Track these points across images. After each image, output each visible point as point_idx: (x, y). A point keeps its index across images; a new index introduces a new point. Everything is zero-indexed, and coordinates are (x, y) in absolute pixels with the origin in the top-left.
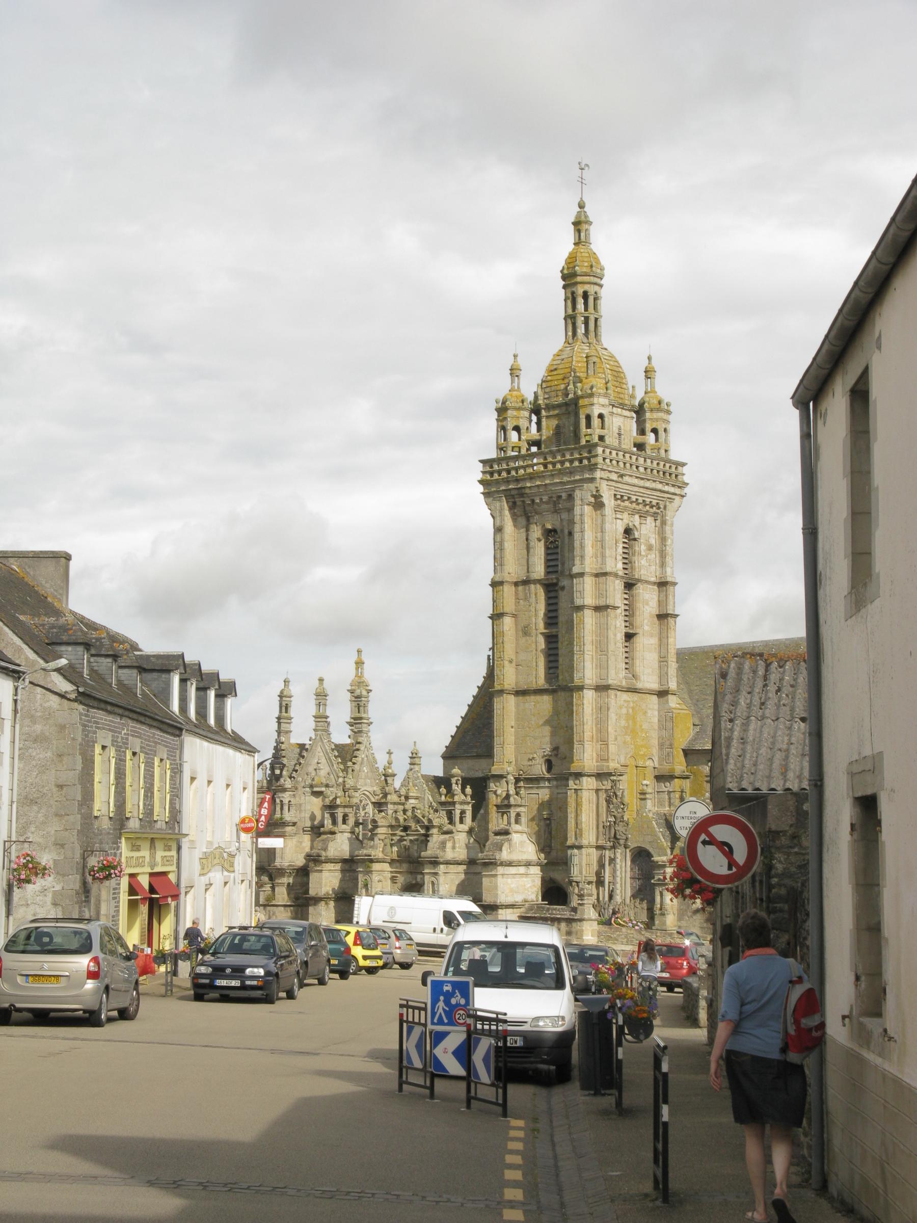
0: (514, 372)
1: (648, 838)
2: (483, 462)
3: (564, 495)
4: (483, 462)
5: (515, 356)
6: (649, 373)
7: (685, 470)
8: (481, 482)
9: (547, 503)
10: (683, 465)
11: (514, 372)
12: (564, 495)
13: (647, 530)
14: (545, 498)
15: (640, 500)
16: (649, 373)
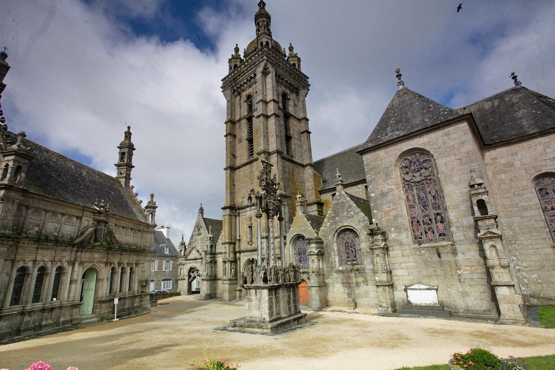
0: (237, 50)
1: (303, 228)
2: (222, 80)
3: (252, 75)
4: (222, 80)
5: (237, 45)
6: (291, 49)
7: (308, 80)
8: (222, 87)
9: (246, 83)
10: (308, 78)
11: (237, 50)
12: (252, 75)
13: (292, 96)
14: (245, 81)
15: (289, 82)
16: (291, 49)
